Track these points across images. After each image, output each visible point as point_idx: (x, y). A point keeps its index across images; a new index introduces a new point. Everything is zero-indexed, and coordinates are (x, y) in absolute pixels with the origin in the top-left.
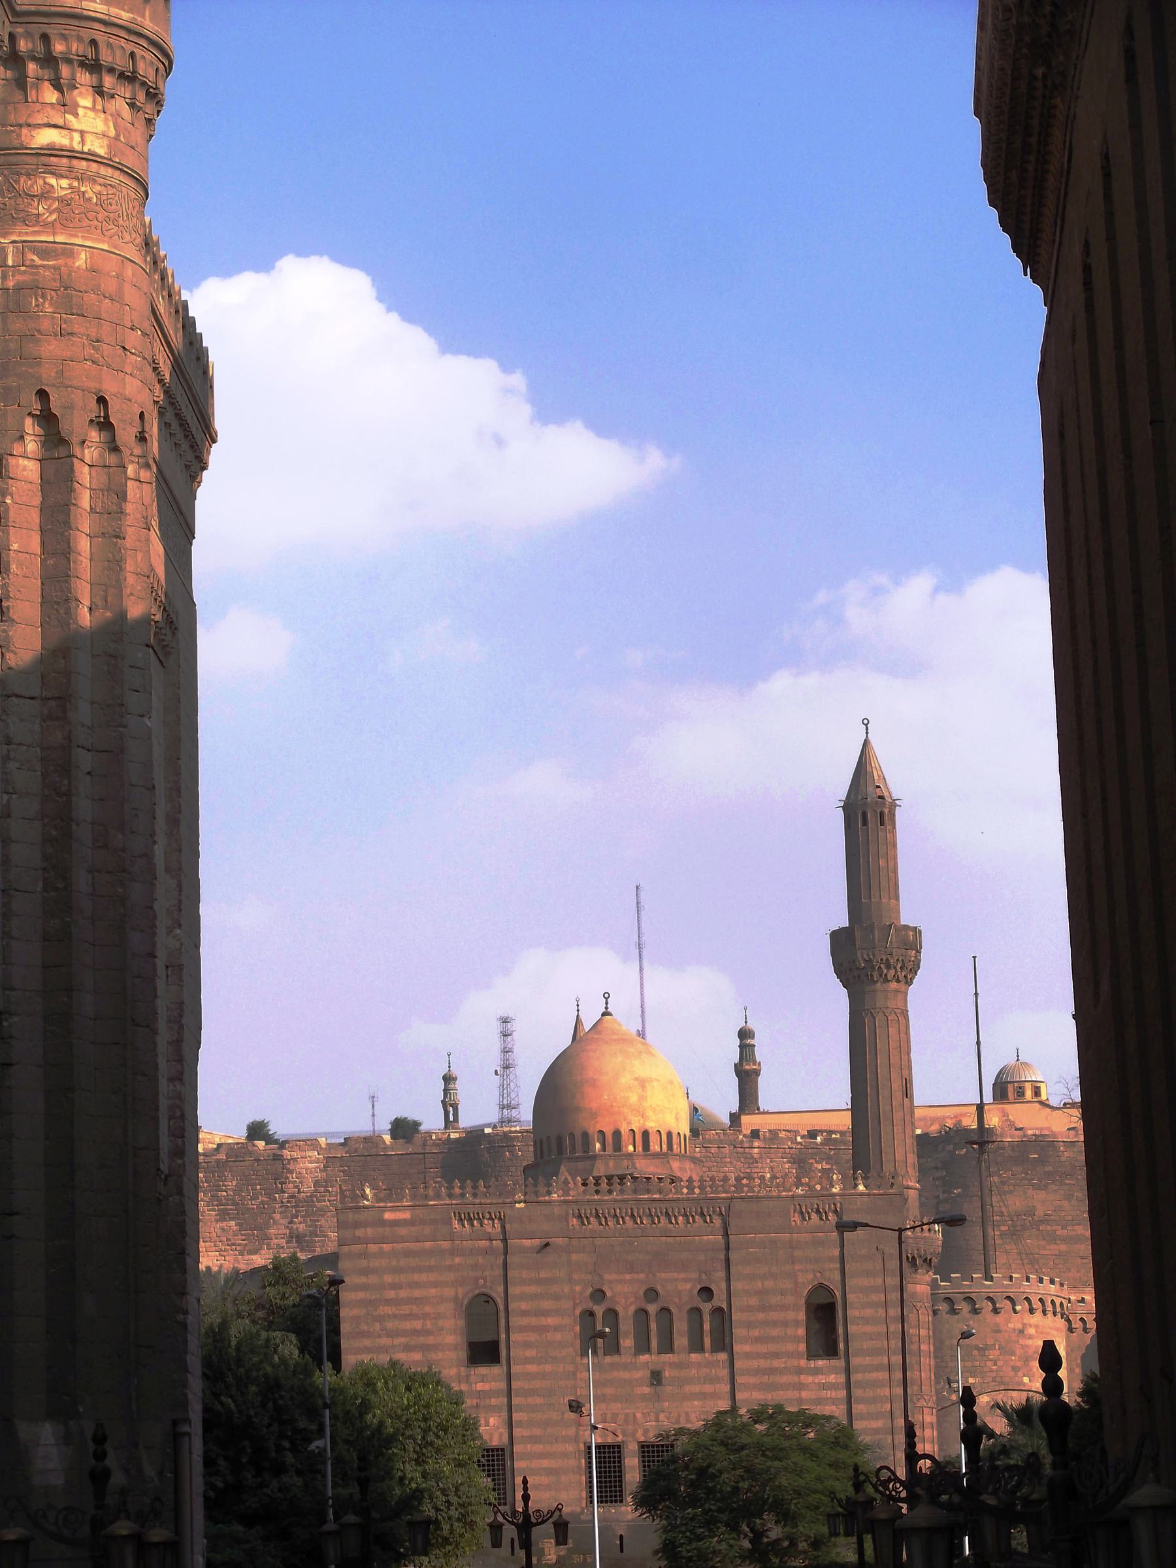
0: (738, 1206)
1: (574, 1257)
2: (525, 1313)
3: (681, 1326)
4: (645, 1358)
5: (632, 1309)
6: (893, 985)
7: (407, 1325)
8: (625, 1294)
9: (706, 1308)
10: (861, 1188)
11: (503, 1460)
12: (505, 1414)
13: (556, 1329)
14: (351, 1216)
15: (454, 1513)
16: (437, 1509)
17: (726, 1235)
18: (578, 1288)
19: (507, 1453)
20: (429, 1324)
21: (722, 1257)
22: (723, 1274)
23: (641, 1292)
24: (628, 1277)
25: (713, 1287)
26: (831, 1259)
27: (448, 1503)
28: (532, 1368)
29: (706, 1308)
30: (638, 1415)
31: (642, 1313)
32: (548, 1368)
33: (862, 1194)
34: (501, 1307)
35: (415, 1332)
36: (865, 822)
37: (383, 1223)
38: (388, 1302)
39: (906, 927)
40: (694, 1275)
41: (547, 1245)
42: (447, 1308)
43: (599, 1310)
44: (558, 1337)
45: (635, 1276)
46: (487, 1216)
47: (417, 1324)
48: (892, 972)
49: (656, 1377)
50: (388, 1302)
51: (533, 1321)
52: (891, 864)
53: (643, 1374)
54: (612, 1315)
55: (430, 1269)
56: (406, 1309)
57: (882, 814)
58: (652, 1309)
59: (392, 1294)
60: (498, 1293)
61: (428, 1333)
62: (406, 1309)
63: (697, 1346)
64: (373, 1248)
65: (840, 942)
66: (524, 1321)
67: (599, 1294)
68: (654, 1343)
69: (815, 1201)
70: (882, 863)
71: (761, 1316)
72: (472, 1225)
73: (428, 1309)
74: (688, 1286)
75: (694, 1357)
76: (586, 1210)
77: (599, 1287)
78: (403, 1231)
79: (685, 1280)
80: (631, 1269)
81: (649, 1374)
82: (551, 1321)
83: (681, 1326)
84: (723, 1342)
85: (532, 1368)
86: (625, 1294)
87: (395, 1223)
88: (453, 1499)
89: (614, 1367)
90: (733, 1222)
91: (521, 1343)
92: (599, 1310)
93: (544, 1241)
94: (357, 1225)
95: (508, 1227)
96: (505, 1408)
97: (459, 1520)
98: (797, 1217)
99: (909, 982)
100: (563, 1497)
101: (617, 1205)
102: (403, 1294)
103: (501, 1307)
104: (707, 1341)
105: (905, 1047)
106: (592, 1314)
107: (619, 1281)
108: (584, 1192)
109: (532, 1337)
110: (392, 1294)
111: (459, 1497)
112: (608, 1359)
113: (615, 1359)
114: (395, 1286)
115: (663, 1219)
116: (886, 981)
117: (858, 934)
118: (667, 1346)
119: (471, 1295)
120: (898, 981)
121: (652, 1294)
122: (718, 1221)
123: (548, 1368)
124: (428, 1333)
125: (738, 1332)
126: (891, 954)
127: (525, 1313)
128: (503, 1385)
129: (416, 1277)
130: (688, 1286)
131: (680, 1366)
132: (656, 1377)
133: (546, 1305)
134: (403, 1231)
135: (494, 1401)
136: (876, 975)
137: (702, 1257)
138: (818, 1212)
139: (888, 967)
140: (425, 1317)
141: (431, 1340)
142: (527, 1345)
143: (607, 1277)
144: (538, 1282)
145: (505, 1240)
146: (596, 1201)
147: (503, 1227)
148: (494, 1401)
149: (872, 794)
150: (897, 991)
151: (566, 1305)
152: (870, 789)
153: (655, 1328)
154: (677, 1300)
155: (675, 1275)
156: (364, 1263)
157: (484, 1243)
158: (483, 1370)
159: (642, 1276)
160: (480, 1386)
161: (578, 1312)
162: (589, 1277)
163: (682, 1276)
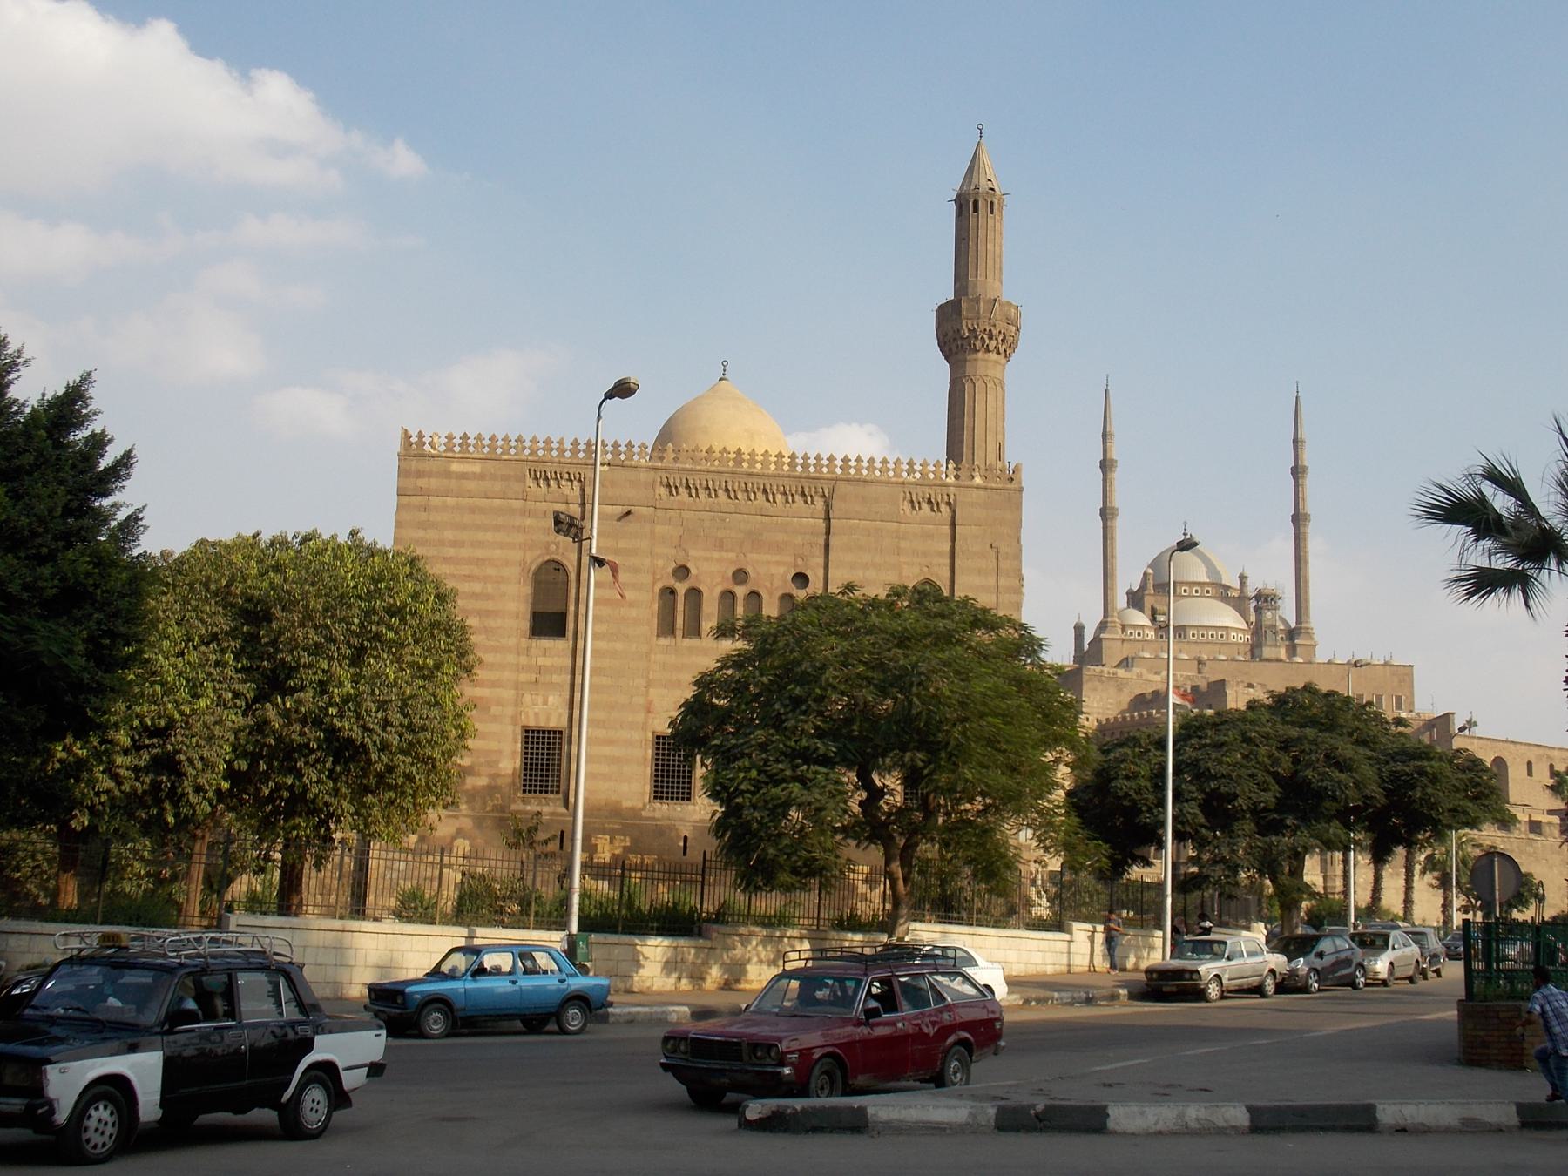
0: (842, 488)
1: (658, 528)
5: (719, 590)
6: (993, 356)
8: (711, 576)
10: (978, 480)
12: (567, 694)
14: (414, 464)
15: (393, 739)
16: (365, 728)
17: (828, 519)
18: (660, 563)
19: (565, 735)
20: (490, 588)
21: (822, 541)
22: (821, 560)
24: (716, 555)
25: (809, 573)
26: (940, 554)
27: (386, 723)
31: (728, 595)
32: (619, 646)
33: (978, 487)
34: (573, 576)
36: (976, 210)
37: (448, 474)
38: (446, 560)
39: (1009, 304)
40: (790, 559)
41: (629, 513)
42: (513, 572)
45: (724, 554)
48: (994, 343)
50: (446, 560)
54: (695, 594)
55: (497, 528)
56: (465, 570)
59: (451, 552)
61: (488, 597)
62: (465, 570)
64: (435, 501)
65: (948, 316)
67: (682, 572)
69: (927, 490)
73: (490, 571)
74: (782, 570)
76: (676, 479)
78: (471, 485)
79: (778, 563)
80: (720, 545)
86: (711, 576)
87: (463, 476)
88: (396, 718)
89: (690, 650)
90: (837, 506)
93: (626, 509)
94: (420, 474)
96: (567, 687)
97: (406, 753)
98: (907, 506)
99: (1007, 357)
100: (624, 788)
101: (710, 477)
102: (465, 552)
103: (573, 576)
105: (1000, 415)
106: (673, 592)
107: (706, 559)
110: (451, 552)
111: (406, 715)
112: (688, 642)
113: (694, 642)
114: (455, 544)
115: (760, 495)
116: (988, 351)
119: (540, 560)
121: (741, 576)
122: (820, 504)
123: (619, 646)
124: (488, 597)
128: (568, 662)
129: (480, 536)
130: (782, 570)
134: (471, 485)
135: (555, 678)
136: (978, 344)
137: (799, 540)
139: (991, 338)
140: (486, 579)
141: (490, 605)
143: (692, 553)
147: (583, 490)
148: (555, 678)
151: (646, 579)
152: (983, 182)
155: (769, 557)
156: (423, 516)
158: (546, 643)
159: (732, 555)
160: (541, 661)
161: (657, 588)
162: (674, 551)
163: (777, 558)
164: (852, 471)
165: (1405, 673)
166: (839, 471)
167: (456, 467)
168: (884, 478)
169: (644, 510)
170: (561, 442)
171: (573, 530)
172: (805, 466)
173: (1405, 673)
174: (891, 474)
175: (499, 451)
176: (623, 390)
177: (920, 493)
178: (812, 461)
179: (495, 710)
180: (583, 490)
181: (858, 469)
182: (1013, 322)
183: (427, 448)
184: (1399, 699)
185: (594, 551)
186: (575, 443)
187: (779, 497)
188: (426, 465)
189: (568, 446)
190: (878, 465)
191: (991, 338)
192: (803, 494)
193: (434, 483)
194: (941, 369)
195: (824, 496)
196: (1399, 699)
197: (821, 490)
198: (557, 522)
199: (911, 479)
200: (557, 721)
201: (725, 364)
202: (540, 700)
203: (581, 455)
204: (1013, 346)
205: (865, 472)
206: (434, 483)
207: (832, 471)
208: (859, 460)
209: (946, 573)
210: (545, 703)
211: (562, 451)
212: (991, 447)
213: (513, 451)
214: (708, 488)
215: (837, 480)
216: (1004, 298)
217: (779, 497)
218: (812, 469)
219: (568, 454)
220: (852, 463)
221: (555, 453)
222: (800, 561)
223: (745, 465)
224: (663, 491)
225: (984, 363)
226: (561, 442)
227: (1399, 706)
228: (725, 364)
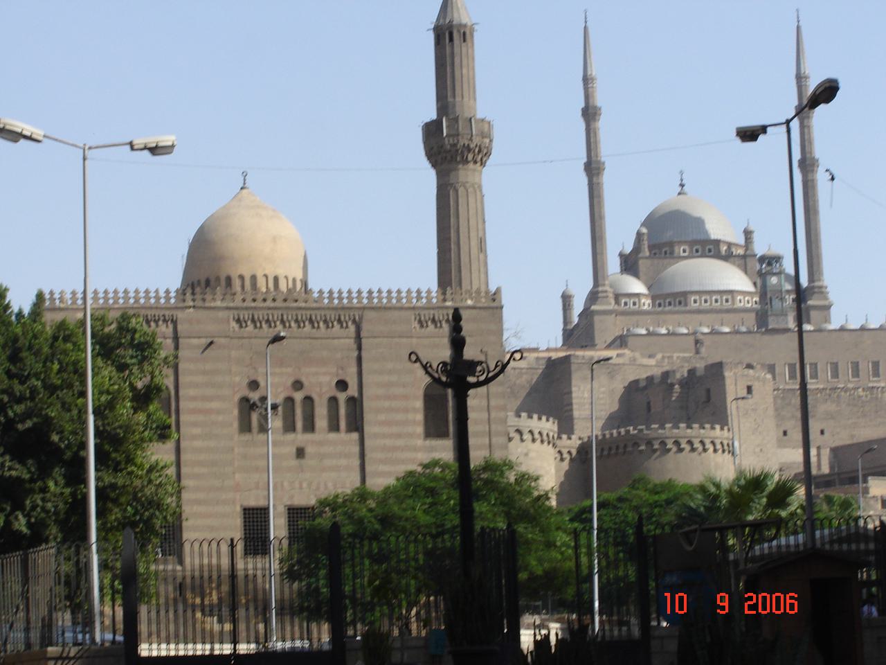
0: (369, 315)
2: (194, 399)
3: (321, 412)
4: (290, 437)
9: (342, 397)
13: (218, 412)
18: (237, 379)
23: (290, 382)
25: (348, 380)
28: (198, 444)
29: (342, 397)
30: (286, 484)
40: (334, 370)
41: (211, 343)
45: (284, 370)
49: (300, 453)
53: (292, 450)
58: (298, 396)
63: (334, 427)
66: (192, 405)
68: (299, 424)
71: (387, 404)
75: (333, 436)
76: (245, 315)
77: (253, 378)
81: (294, 450)
82: (215, 405)
83: (321, 412)
84: (356, 423)
85: (198, 444)
90: (366, 328)
93: (209, 340)
95: (179, 327)
98: (416, 325)
101: (270, 312)
104: (343, 424)
118: (310, 426)
121: (298, 385)
122: (352, 328)
125: (368, 417)
127: (194, 399)
131: (320, 443)
132: (300, 453)
137: (339, 355)
142: (195, 424)
144: (204, 373)
153: (298, 413)
154: (318, 390)
159: (289, 370)
169: (223, 341)
170: (157, 291)
172: (340, 298)
177: (426, 315)
181: (380, 299)
182: (487, 135)
194: (429, 176)
199: (419, 304)
201: (245, 175)
204: (488, 154)
205: (385, 301)
207: (360, 302)
211: (157, 298)
212: (474, 243)
215: (364, 308)
216: (480, 115)
222: (340, 372)
224: (234, 324)
225: (465, 174)
228: (245, 175)
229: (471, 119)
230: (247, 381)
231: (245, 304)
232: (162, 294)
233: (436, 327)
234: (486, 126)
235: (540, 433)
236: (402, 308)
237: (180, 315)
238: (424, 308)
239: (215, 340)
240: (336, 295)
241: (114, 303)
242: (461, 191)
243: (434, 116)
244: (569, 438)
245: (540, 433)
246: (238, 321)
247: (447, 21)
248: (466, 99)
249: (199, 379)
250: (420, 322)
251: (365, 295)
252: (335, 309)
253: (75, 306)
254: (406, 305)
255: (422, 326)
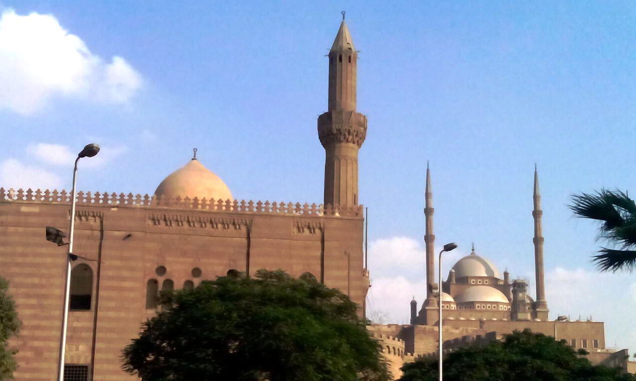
0: (257, 220)
1: (148, 245)
6: (351, 145)
7: (29, 281)
10: (337, 215)
11: (86, 374)
12: (91, 344)
13: (131, 290)
17: (249, 238)
18: (148, 265)
20: (44, 281)
21: (245, 251)
22: (245, 263)
23: (190, 270)
24: (182, 260)
28: (112, 314)
32: (123, 314)
33: (337, 219)
34: (95, 274)
35: (34, 286)
37: (19, 213)
38: (18, 265)
39: (360, 114)
41: (129, 236)
43: (161, 280)
44: (132, 295)
46: (91, 214)
47: (36, 280)
50: (18, 265)
51: (115, 283)
52: (353, 84)
56: (27, 270)
57: (350, 58)
60: (94, 266)
61: (42, 286)
62: (27, 270)
64: (11, 229)
65: (325, 122)
67: (161, 270)
69: (308, 221)
70: (349, 81)
72: (81, 219)
73: (44, 271)
76: (158, 215)
80: (184, 254)
82: (127, 284)
85: (112, 314)
90: (254, 230)
91: (105, 295)
92: (161, 280)
93: (128, 233)
95: (104, 222)
96: (91, 340)
98: (295, 230)
99: (359, 145)
102: (29, 260)
103: (95, 274)
105: (355, 178)
106: (154, 282)
108: (158, 204)
109: (114, 294)
110: (20, 260)
114: (23, 255)
115: (209, 225)
116: (348, 141)
117: (334, 115)
120: (354, 143)
122: (244, 229)
124: (42, 286)
126: (351, 127)
127: (111, 278)
128: (91, 324)
133: (125, 273)
134: (33, 220)
135: (84, 335)
136: (342, 138)
138: (309, 228)
140: (41, 276)
141: (43, 291)
142: (110, 299)
143: (168, 259)
144: (122, 258)
145: (102, 231)
146: (165, 210)
147: (102, 222)
148: (84, 335)
149: (345, 46)
150: (353, 148)
151: (139, 274)
157: (88, 232)
159: (191, 260)
161: (146, 280)
164: (263, 210)
165: (598, 328)
166: (255, 210)
167: (24, 209)
168: (282, 214)
169: (139, 234)
170: (89, 194)
171: (59, 239)
173: (598, 328)
174: (286, 211)
175: (51, 199)
176: (90, 151)
178: (239, 204)
179: (46, 354)
180: (102, 222)
181: (267, 209)
182: (363, 124)
183: (6, 198)
184: (596, 342)
185: (71, 251)
186: (97, 194)
187: (220, 226)
188: (5, 208)
189: (93, 196)
190: (278, 206)
191: (349, 133)
192: (234, 224)
193: (10, 219)
194: (322, 152)
195: (246, 225)
196: (596, 342)
197: (243, 220)
198: (48, 234)
199: (298, 214)
200: (83, 359)
201: (195, 150)
202: (74, 347)
203: (101, 201)
204: (363, 138)
205: (271, 210)
206: (10, 219)
207: (251, 210)
208: (267, 203)
209: (318, 269)
210: (77, 349)
211: (89, 199)
212: (350, 198)
213: (59, 200)
214: (177, 221)
215: (254, 215)
217: (220, 226)
218: (239, 209)
219: (93, 201)
220: (263, 205)
221: (85, 201)
222: (232, 263)
223: (200, 206)
224: (150, 222)
225: (347, 149)
226: (89, 194)
227: (596, 345)
228: (195, 150)
229: (351, 112)
230: (156, 267)
231: (160, 207)
232: (93, 196)
233: (310, 232)
234: (362, 119)
235: (394, 348)
236: (284, 217)
237: (105, 212)
238: (301, 217)
239: (132, 233)
240: (232, 204)
241: (52, 201)
242: (342, 161)
243: (327, 110)
244: (412, 355)
245: (394, 348)
246: (153, 219)
247: (339, 48)
248: (348, 101)
249: (117, 263)
250: (298, 228)
251: (255, 205)
252: (231, 214)
253: (20, 202)
254: (288, 215)
255: (299, 231)
